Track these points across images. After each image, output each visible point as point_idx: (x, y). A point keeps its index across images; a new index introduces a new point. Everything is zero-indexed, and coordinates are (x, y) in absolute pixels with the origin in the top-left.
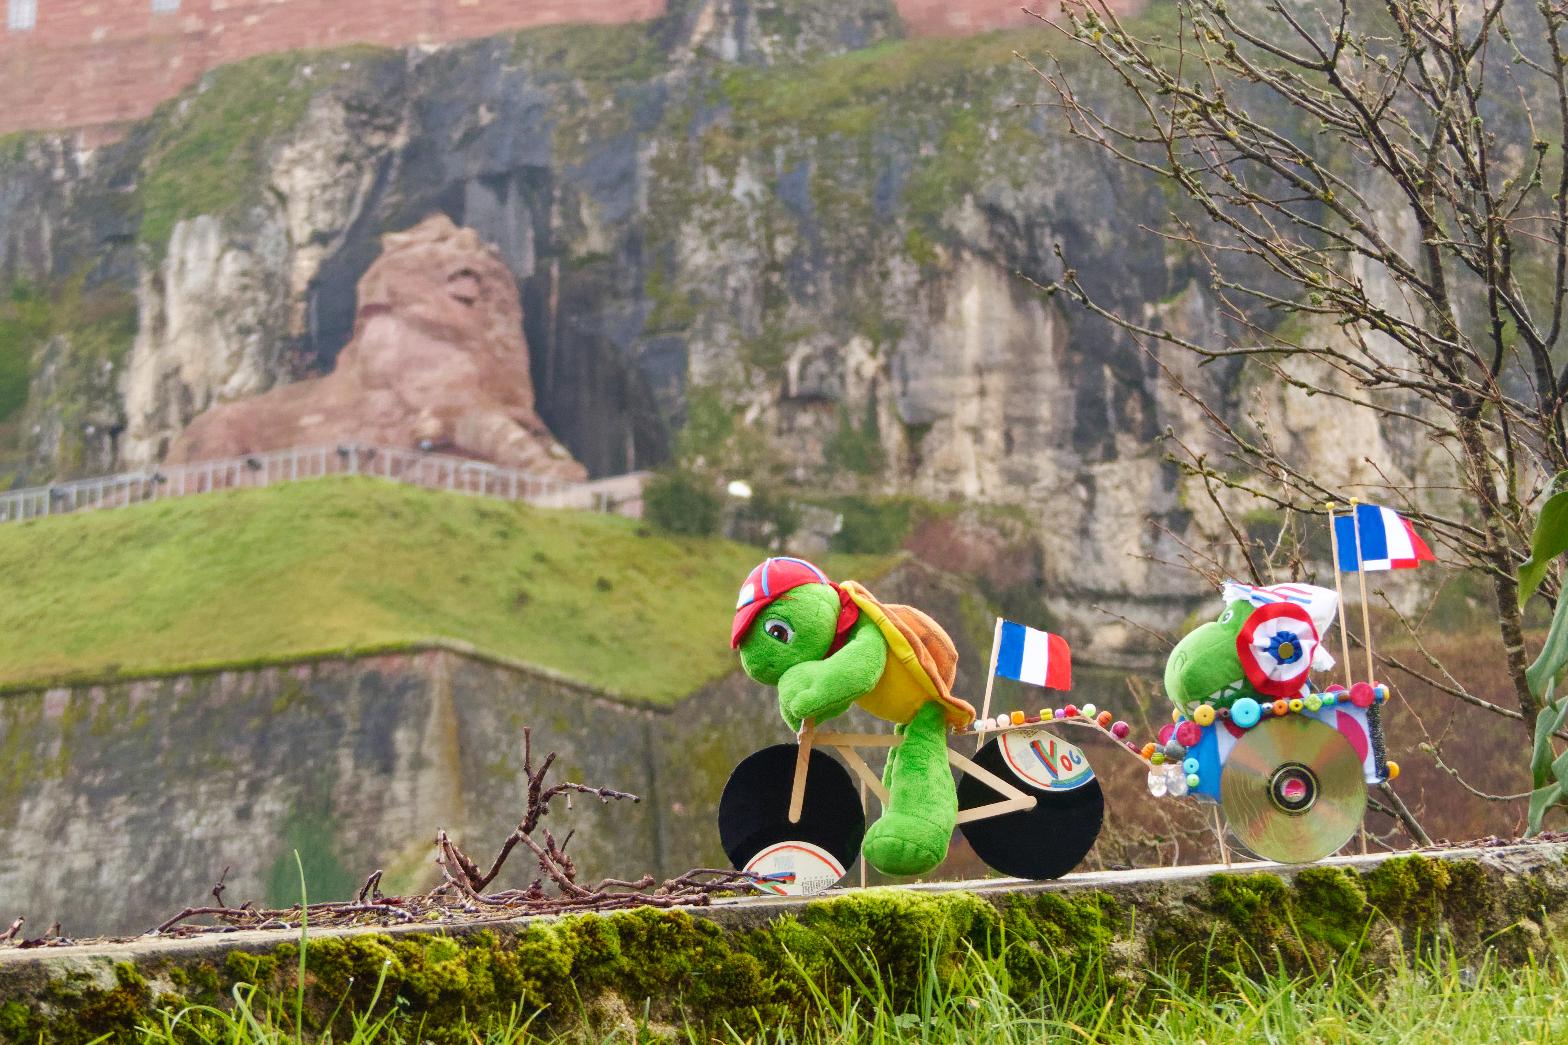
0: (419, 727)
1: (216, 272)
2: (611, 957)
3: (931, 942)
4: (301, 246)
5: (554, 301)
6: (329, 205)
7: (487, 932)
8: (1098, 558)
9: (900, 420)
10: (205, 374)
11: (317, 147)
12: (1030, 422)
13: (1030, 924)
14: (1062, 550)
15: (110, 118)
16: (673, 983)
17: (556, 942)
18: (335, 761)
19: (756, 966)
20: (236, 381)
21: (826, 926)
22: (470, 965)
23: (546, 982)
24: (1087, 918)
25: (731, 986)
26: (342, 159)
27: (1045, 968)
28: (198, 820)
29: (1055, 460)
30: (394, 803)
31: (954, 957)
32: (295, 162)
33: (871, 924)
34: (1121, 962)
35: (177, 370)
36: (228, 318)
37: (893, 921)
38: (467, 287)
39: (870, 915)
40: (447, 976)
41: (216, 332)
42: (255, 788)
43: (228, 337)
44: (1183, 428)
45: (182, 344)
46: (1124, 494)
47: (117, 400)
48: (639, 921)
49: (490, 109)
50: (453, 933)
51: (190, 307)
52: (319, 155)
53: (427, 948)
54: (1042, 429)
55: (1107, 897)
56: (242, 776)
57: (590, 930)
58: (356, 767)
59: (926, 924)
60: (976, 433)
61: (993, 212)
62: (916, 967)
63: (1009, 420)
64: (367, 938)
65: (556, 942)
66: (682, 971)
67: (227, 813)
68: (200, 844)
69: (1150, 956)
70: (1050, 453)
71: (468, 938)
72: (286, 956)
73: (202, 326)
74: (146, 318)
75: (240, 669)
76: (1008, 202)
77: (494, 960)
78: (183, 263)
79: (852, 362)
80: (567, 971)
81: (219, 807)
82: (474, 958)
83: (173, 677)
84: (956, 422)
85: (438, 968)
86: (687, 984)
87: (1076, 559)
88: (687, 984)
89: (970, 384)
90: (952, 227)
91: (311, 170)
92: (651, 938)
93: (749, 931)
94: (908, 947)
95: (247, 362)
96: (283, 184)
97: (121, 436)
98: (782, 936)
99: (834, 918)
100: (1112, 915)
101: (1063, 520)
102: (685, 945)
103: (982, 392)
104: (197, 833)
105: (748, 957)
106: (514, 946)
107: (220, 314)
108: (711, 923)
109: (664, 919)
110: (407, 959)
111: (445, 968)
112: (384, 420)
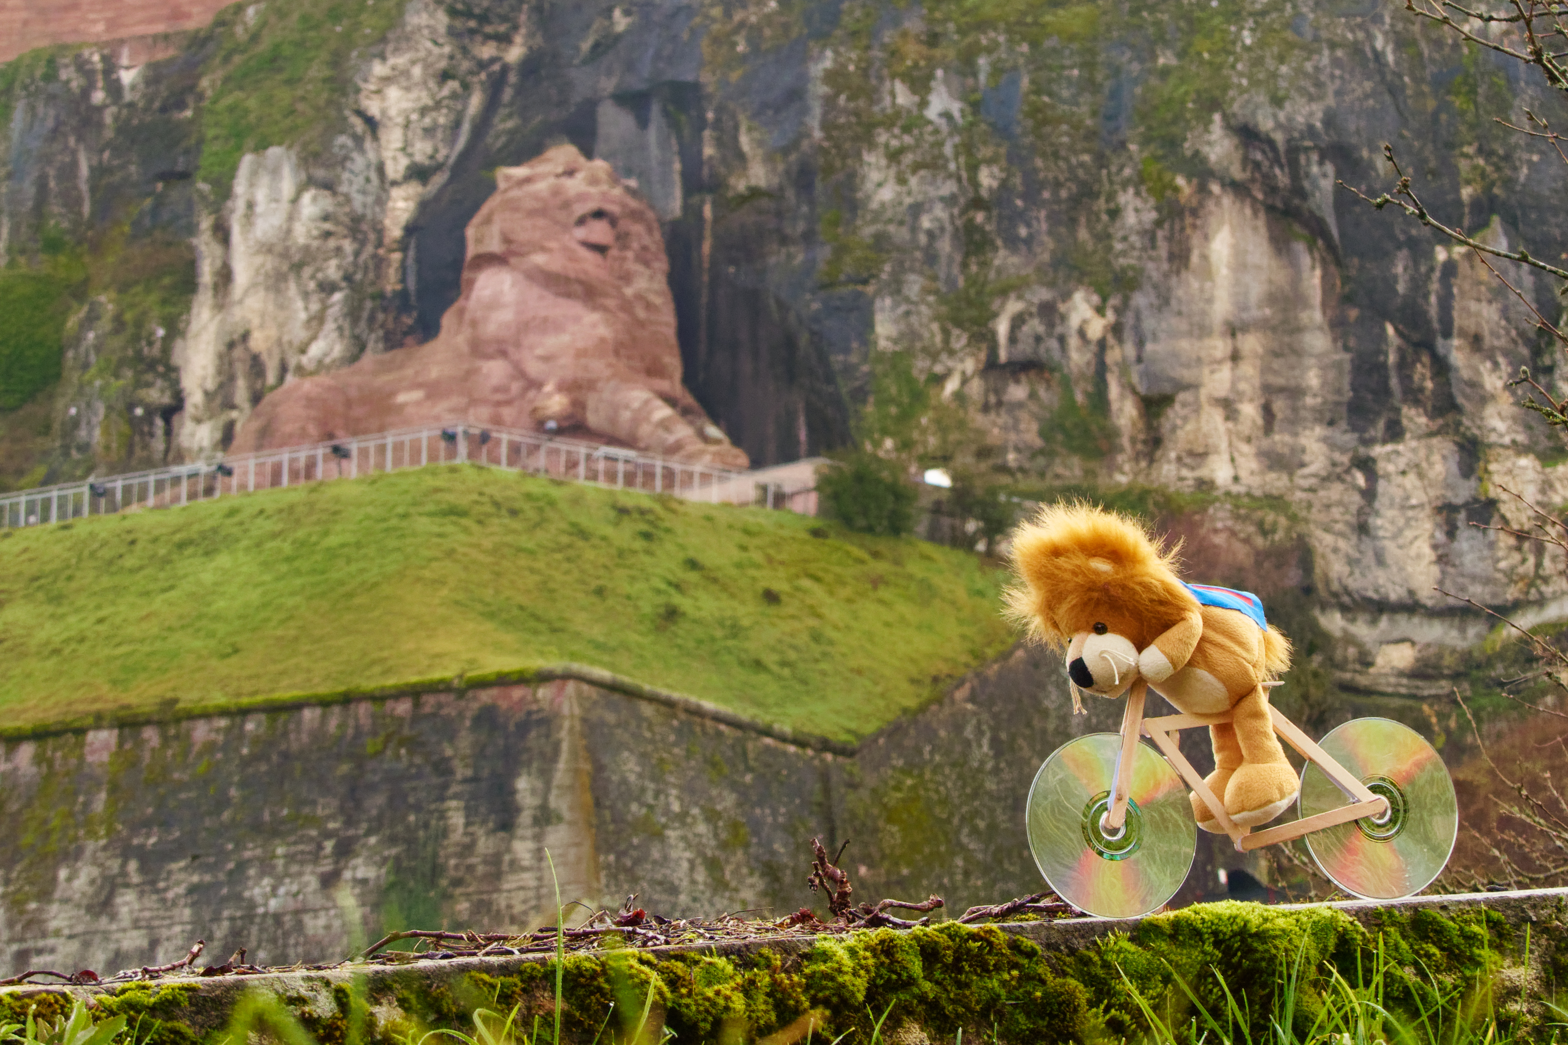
0: (546, 774)
1: (291, 218)
2: (911, 981)
3: (1289, 965)
4: (394, 183)
5: (707, 247)
6: (429, 132)
7: (765, 951)
8: (1380, 560)
9: (1134, 391)
10: (279, 342)
11: (413, 62)
12: (1295, 393)
13: (1404, 945)
14: (1336, 550)
15: (160, 28)
16: (984, 1014)
17: (848, 963)
18: (442, 815)
19: (1082, 994)
20: (316, 349)
21: (1164, 946)
22: (748, 988)
23: (836, 1011)
24: (1471, 939)
25: (1052, 1016)
26: (445, 76)
27: (1424, 998)
28: (274, 889)
29: (1325, 440)
30: (515, 866)
31: (1315, 984)
32: (387, 80)
33: (1217, 944)
34: (1513, 992)
35: (245, 336)
36: (307, 271)
37: (1243, 941)
38: (599, 232)
39: (1215, 933)
40: (721, 1002)
41: (292, 289)
42: (345, 850)
43: (306, 295)
44: (1484, 399)
45: (251, 305)
46: (1411, 481)
47: (172, 375)
48: (943, 939)
49: (627, 13)
50: (725, 952)
51: (259, 260)
52: (417, 71)
53: (696, 969)
54: (1309, 401)
55: (1495, 915)
56: (328, 835)
57: (887, 948)
58: (467, 824)
59: (1282, 944)
60: (1228, 407)
61: (1247, 135)
62: (1271, 995)
63: (1268, 390)
64: (626, 957)
65: (848, 963)
66: (996, 998)
67: (311, 881)
68: (277, 918)
69: (1547, 985)
70: (1319, 430)
71: (744, 957)
72: (532, 978)
73: (275, 283)
74: (207, 273)
75: (325, 703)
76: (1265, 123)
77: (775, 984)
78: (251, 205)
79: (1074, 321)
80: (861, 997)
81: (300, 874)
82: (752, 982)
83: (244, 712)
84: (1204, 393)
85: (710, 993)
86: (1000, 1015)
87: (1351, 562)
88: (1000, 1015)
89: (1220, 346)
90: (1197, 153)
91: (408, 89)
92: (958, 959)
93: (1072, 952)
94: (1261, 972)
95: (330, 326)
96: (373, 108)
97: (176, 419)
98: (1111, 957)
99: (1173, 937)
100: (1501, 936)
101: (1336, 512)
102: (998, 968)
103: (1235, 357)
104: (273, 904)
105: (1073, 982)
106: (797, 968)
107: (297, 268)
108: (1028, 943)
109: (973, 937)
110: (674, 982)
111: (718, 993)
112: (499, 397)
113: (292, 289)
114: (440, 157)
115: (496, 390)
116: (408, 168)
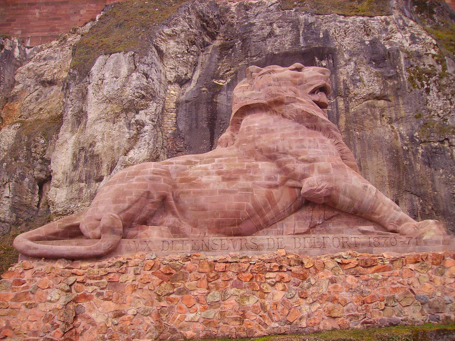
4: (170, 82)
6: (185, 64)
11: (182, 31)
20: (131, 154)
35: (92, 145)
41: (122, 122)
43: (129, 125)
51: (103, 106)
52: (183, 35)
78: (102, 80)
95: (141, 142)
96: (163, 47)
107: (126, 111)
113: (122, 122)
114: (189, 75)
115: (269, 179)
116: (175, 77)
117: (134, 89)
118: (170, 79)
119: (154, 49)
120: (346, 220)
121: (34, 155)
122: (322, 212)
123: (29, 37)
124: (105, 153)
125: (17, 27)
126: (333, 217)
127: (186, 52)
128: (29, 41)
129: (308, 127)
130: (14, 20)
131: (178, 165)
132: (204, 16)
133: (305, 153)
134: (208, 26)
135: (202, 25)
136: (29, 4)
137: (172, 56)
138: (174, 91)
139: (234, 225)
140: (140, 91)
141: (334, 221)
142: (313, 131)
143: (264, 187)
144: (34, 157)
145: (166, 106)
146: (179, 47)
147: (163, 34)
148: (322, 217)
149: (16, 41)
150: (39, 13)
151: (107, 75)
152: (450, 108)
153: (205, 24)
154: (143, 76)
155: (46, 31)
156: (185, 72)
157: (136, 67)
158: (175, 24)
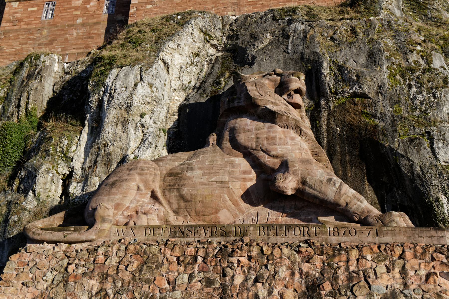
11: (185, 45)
15: (81, 51)
38: (297, 99)
47: (68, 159)
52: (186, 49)
96: (168, 59)
115: (245, 172)
117: (140, 97)
118: (174, 87)
119: (160, 62)
120: (315, 211)
121: (59, 154)
122: (293, 203)
123: (67, 54)
124: (115, 151)
125: (58, 45)
126: (303, 207)
127: (190, 63)
128: (67, 57)
129: (280, 126)
130: (56, 40)
131: (169, 162)
132: (206, 30)
133: (276, 149)
134: (210, 39)
135: (205, 39)
136: (68, 26)
137: (177, 67)
138: (178, 98)
139: (213, 214)
140: (144, 98)
141: (304, 211)
142: (285, 130)
143: (240, 180)
144: (59, 156)
145: (170, 111)
146: (184, 59)
147: (168, 48)
148: (293, 207)
149: (56, 57)
150: (77, 33)
151: (118, 86)
152: (433, 102)
153: (207, 37)
154: (148, 85)
155: (80, 48)
156: (189, 81)
157: (141, 78)
158: (179, 39)
